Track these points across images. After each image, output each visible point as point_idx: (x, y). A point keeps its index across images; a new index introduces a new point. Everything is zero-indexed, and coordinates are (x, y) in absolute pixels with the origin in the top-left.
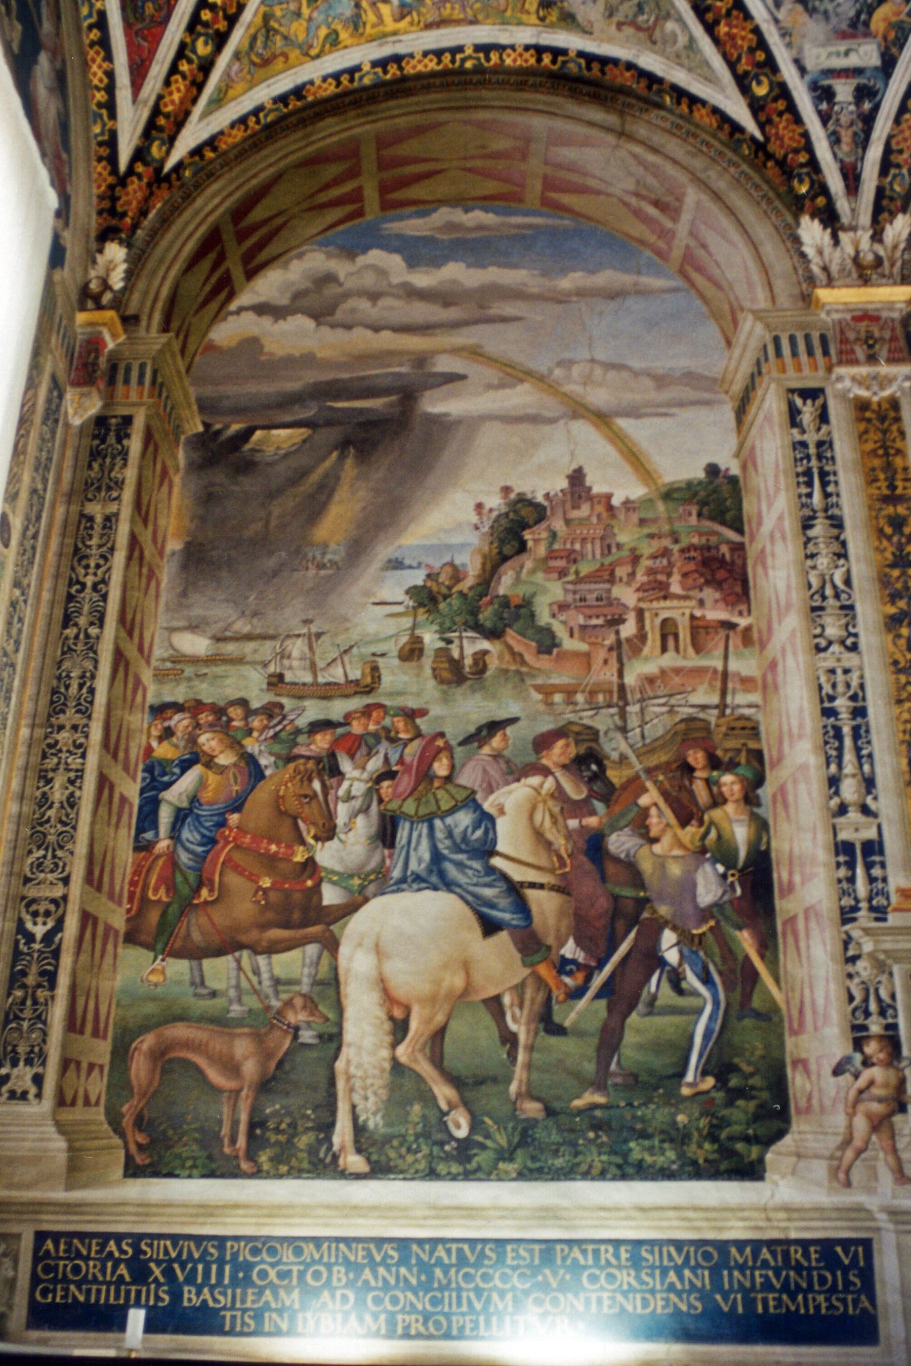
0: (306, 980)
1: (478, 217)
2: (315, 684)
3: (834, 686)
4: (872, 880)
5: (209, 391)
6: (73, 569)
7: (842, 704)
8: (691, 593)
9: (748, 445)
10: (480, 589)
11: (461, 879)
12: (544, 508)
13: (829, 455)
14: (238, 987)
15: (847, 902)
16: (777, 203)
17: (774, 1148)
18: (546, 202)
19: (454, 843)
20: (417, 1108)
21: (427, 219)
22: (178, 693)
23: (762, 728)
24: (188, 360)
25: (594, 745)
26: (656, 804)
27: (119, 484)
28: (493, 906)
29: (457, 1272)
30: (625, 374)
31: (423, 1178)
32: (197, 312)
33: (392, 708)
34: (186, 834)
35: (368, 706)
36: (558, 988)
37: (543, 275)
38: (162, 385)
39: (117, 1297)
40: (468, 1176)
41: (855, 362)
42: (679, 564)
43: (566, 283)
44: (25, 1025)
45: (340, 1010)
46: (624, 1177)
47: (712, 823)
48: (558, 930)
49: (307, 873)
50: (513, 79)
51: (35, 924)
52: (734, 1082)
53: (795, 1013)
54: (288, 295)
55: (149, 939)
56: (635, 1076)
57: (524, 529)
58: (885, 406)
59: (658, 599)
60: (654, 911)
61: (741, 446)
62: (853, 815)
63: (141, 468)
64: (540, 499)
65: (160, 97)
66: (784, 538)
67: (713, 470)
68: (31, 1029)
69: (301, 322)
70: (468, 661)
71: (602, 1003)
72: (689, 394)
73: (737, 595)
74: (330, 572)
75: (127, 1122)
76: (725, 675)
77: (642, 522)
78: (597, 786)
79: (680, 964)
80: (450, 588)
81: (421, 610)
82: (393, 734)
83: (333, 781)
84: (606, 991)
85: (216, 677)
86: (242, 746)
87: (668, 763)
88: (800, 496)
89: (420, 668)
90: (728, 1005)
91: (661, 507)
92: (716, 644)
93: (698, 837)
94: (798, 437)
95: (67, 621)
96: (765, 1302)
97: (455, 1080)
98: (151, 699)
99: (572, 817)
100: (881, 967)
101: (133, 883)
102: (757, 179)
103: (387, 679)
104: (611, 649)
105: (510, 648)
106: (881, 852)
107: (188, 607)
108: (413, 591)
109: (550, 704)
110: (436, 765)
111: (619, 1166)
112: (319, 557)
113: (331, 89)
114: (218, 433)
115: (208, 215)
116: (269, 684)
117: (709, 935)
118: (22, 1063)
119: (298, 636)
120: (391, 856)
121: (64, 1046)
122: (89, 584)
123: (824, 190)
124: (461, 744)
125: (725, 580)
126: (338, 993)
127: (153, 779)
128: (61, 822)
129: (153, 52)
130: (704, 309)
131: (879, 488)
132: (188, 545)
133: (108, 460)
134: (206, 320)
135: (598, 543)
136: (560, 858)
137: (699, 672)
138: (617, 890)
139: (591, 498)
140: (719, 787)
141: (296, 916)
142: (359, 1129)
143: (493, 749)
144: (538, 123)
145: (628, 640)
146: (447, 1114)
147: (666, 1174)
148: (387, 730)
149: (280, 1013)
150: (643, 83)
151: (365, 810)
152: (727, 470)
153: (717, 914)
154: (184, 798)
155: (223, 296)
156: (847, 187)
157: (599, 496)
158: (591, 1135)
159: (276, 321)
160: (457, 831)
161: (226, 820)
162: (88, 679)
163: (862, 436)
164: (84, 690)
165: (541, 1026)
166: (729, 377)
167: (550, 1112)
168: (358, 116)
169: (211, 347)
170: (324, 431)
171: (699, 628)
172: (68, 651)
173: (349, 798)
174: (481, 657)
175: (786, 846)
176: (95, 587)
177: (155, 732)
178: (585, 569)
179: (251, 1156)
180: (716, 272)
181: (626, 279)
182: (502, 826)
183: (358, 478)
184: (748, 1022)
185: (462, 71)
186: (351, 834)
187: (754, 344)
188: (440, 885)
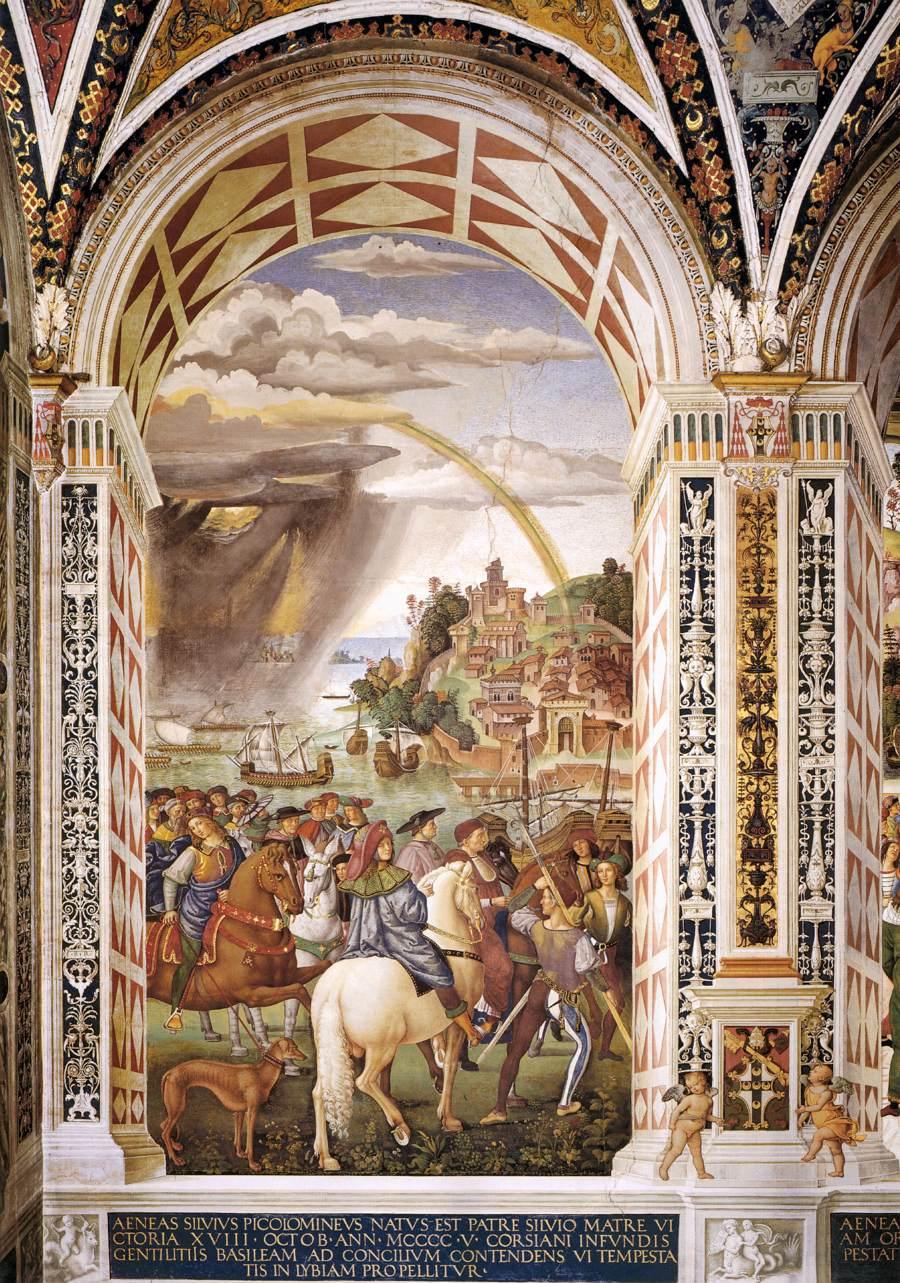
2: (280, 774)
3: (692, 785)
4: (704, 952)
6: (63, 654)
7: (697, 801)
8: (584, 694)
9: (642, 541)
10: (413, 684)
11: (401, 948)
13: (710, 553)
14: (238, 1032)
15: (685, 969)
16: (692, 248)
17: (618, 1153)
22: (168, 781)
23: (633, 823)
25: (501, 834)
26: (548, 887)
27: (94, 563)
28: (424, 970)
29: (402, 1237)
30: (541, 455)
31: (378, 1174)
32: (142, 362)
34: (187, 907)
35: (323, 795)
37: (468, 331)
39: (171, 1256)
40: (408, 1173)
42: (577, 664)
43: (490, 342)
44: (81, 1061)
47: (589, 903)
48: (473, 990)
49: (284, 941)
51: (77, 981)
52: (594, 1105)
54: (230, 344)
56: (525, 1101)
57: (449, 625)
62: (696, 899)
64: (463, 593)
67: (611, 566)
69: (242, 378)
70: (404, 755)
75: (165, 1135)
76: (608, 770)
79: (561, 1018)
81: (365, 704)
82: (345, 822)
85: (198, 766)
86: (225, 831)
87: (559, 852)
88: (681, 597)
89: (365, 761)
91: (565, 604)
92: (602, 742)
94: (687, 533)
96: (606, 1254)
97: (401, 1105)
100: (705, 1021)
101: (149, 948)
105: (437, 743)
106: (714, 930)
107: (168, 696)
108: (357, 685)
110: (380, 850)
111: (513, 1166)
112: (276, 648)
114: (177, 508)
118: (82, 1091)
119: (264, 727)
120: (347, 928)
121: (112, 1078)
122: (80, 671)
124: (398, 832)
126: (312, 1037)
127: (156, 859)
128: (86, 895)
129: (65, 52)
131: (748, 590)
133: (79, 535)
134: (153, 374)
136: (474, 929)
137: (588, 768)
138: (517, 959)
141: (278, 977)
142: (332, 1139)
146: (394, 1128)
151: (325, 888)
154: (182, 875)
155: (165, 341)
156: (762, 242)
158: (494, 1144)
160: (397, 908)
162: (91, 765)
163: (740, 537)
164: (89, 776)
165: (460, 1064)
167: (466, 1127)
168: (286, 101)
170: (272, 509)
171: (590, 728)
176: (85, 671)
177: (153, 817)
178: (500, 666)
184: (607, 1061)
187: (656, 427)
188: (386, 953)
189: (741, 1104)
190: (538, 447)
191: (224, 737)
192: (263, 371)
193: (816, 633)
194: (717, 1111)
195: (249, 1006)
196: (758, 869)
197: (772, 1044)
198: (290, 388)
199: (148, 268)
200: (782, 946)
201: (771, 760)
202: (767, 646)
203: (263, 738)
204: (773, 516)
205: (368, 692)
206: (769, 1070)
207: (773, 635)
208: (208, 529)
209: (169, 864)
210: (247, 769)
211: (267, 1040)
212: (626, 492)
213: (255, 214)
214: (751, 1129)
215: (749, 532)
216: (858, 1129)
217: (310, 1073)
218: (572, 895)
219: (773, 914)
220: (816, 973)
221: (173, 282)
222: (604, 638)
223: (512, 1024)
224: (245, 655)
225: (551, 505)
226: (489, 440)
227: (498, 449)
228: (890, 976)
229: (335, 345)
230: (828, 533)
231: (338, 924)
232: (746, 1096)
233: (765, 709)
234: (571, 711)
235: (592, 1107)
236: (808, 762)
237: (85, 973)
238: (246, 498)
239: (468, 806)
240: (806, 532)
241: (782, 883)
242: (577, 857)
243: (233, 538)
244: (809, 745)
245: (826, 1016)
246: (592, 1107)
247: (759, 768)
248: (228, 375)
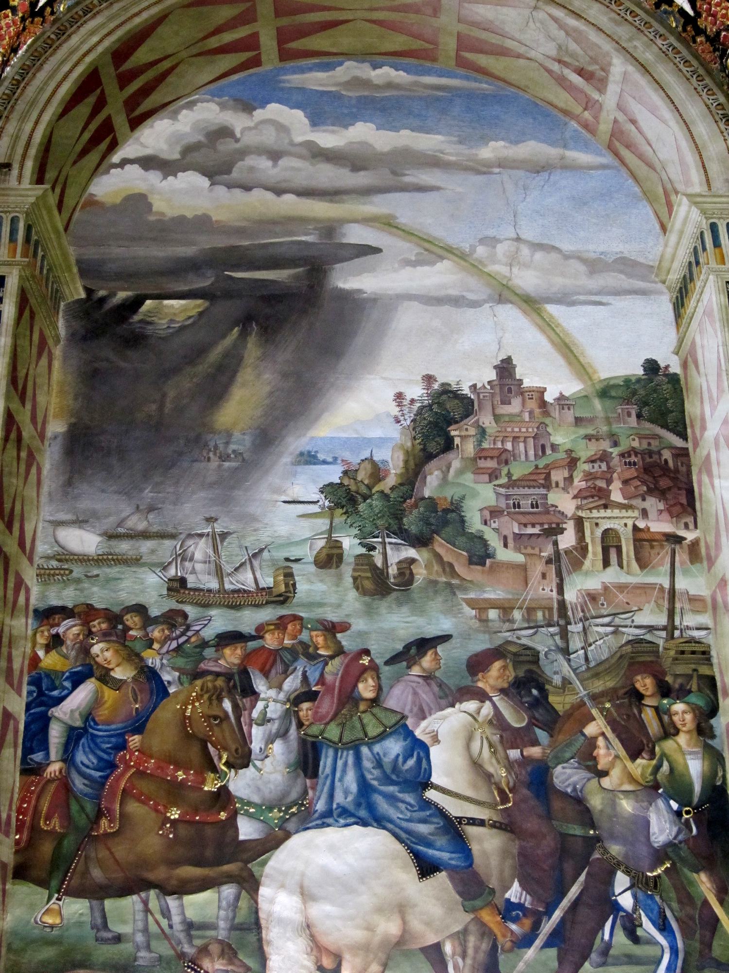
0: (222, 924)
2: (222, 590)
5: (92, 253)
8: (634, 502)
9: (687, 342)
10: (404, 489)
12: (472, 402)
14: (146, 930)
16: (708, 81)
18: (462, 63)
19: (384, 772)
21: (330, 73)
22: (66, 597)
23: (713, 653)
24: (66, 215)
25: (534, 667)
26: (603, 734)
30: (554, 255)
32: (75, 163)
33: (310, 620)
34: (80, 757)
36: (504, 936)
38: (37, 243)
42: (619, 470)
47: (664, 755)
48: (502, 872)
54: (179, 149)
55: (44, 875)
57: (449, 424)
59: (597, 508)
60: (606, 851)
61: (681, 342)
64: (466, 391)
67: (651, 367)
70: (393, 570)
71: (553, 952)
72: (622, 281)
73: (682, 505)
74: (234, 464)
76: (672, 592)
77: (578, 421)
78: (539, 714)
79: (635, 910)
80: (369, 487)
81: (340, 511)
82: (311, 650)
83: (247, 701)
84: (556, 938)
85: (108, 580)
86: (142, 659)
87: (614, 690)
89: (340, 577)
90: (687, 954)
91: (597, 404)
93: (650, 770)
99: (513, 748)
101: (20, 811)
102: (685, 53)
103: (302, 587)
104: (549, 562)
105: (439, 557)
107: (76, 498)
108: (328, 489)
109: (484, 621)
110: (361, 686)
112: (221, 447)
114: (102, 300)
115: (85, 55)
116: (169, 589)
117: (665, 878)
119: (201, 536)
124: (387, 663)
125: (669, 489)
126: (260, 940)
127: (41, 693)
130: (637, 189)
134: (86, 174)
135: (531, 441)
139: (522, 393)
140: (670, 716)
141: (209, 853)
143: (424, 670)
145: (567, 552)
148: (305, 645)
151: (283, 734)
152: (667, 367)
153: (671, 855)
154: (77, 715)
155: (103, 146)
157: (531, 390)
159: (165, 178)
160: (387, 760)
161: (125, 742)
166: (666, 264)
169: (92, 203)
174: (407, 566)
177: (41, 640)
178: (518, 471)
181: (552, 152)
182: (436, 754)
183: (263, 358)
186: (267, 761)
187: (691, 230)
188: (371, 821)
190: (554, 248)
203: (200, 549)
208: (141, 321)
209: (60, 700)
210: (176, 585)
212: (661, 293)
213: (214, 42)
221: (116, 98)
222: (652, 441)
223: (563, 921)
224: (181, 454)
225: (573, 304)
226: (491, 242)
227: (501, 249)
229: (304, 152)
231: (300, 781)
238: (190, 291)
239: (484, 632)
242: (640, 697)
243: (171, 331)
248: (175, 176)
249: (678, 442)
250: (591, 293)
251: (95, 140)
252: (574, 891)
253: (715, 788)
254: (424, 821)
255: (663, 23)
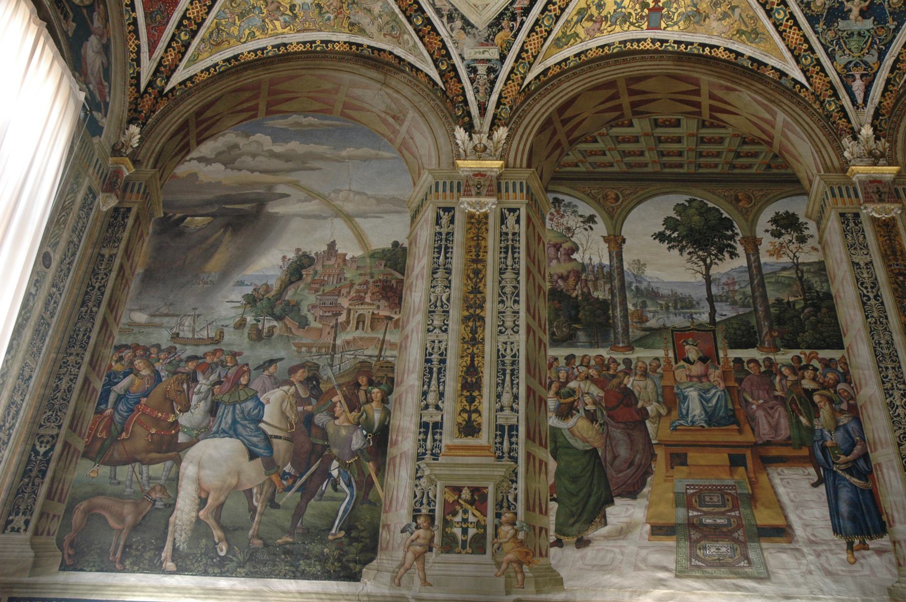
1: (310, 119)
3: (433, 348)
4: (434, 440)
7: (435, 357)
9: (414, 233)
11: (244, 433)
12: (314, 259)
14: (131, 480)
15: (421, 450)
17: (367, 566)
18: (343, 114)
20: (204, 541)
22: (129, 340)
23: (396, 367)
27: (120, 240)
28: (256, 446)
31: (201, 575)
34: (120, 407)
40: (222, 574)
41: (471, 196)
43: (344, 153)
44: (26, 495)
45: (177, 492)
46: (295, 578)
47: (365, 411)
50: (338, 56)
52: (353, 534)
53: (388, 502)
56: (308, 529)
58: (482, 217)
62: (431, 409)
63: (131, 233)
64: (313, 255)
65: (162, 58)
66: (422, 278)
67: (396, 244)
68: (29, 497)
69: (219, 166)
70: (265, 331)
71: (299, 494)
76: (383, 341)
83: (193, 384)
84: (302, 488)
85: (147, 334)
87: (349, 382)
89: (243, 333)
90: (357, 497)
91: (368, 260)
94: (438, 230)
95: (83, 303)
97: (223, 528)
98: (116, 342)
100: (432, 482)
101: (91, 429)
102: (442, 107)
103: (227, 338)
104: (332, 327)
105: (286, 325)
106: (441, 428)
109: (299, 352)
111: (293, 572)
113: (252, 57)
114: (170, 217)
121: (44, 505)
123: (469, 114)
127: (110, 380)
130: (407, 167)
132: (146, 271)
137: (372, 339)
138: (315, 441)
141: (164, 447)
142: (175, 549)
144: (347, 77)
147: (315, 577)
148: (222, 361)
149: (149, 493)
150: (397, 61)
151: (205, 399)
157: (341, 254)
158: (283, 556)
160: (246, 410)
162: (88, 331)
167: (266, 545)
168: (264, 70)
169: (174, 176)
171: (375, 319)
172: (81, 318)
173: (199, 392)
174: (271, 329)
175: (397, 423)
176: (99, 289)
177: (114, 358)
178: (328, 289)
179: (122, 562)
180: (415, 149)
182: (267, 408)
185: (316, 52)
187: (427, 185)
189: (453, 537)
191: (166, 320)
192: (228, 163)
193: (509, 275)
194: (437, 540)
195: (143, 464)
196: (471, 394)
197: (476, 497)
198: (240, 170)
199: (185, 125)
200: (484, 438)
201: (481, 336)
202: (481, 281)
204: (486, 223)
205: (251, 300)
206: (473, 514)
207: (484, 276)
209: (117, 383)
211: (148, 485)
213: (239, 108)
214: (460, 553)
215: (473, 230)
216: (534, 555)
217: (171, 506)
218: (353, 405)
219: (479, 420)
220: (506, 455)
225: (368, 217)
226: (337, 191)
227: (341, 194)
228: (555, 458)
230: (516, 231)
232: (458, 531)
233: (478, 311)
234: (366, 311)
235: (352, 535)
236: (503, 338)
237: (48, 442)
240: (504, 230)
241: (485, 404)
242: (360, 385)
244: (504, 330)
245: (513, 482)
246: (352, 535)
247: (473, 340)
249: (399, 276)
250: (376, 213)
251: (181, 150)
252: (313, 468)
253: (384, 425)
254: (255, 436)
255: (435, 94)
